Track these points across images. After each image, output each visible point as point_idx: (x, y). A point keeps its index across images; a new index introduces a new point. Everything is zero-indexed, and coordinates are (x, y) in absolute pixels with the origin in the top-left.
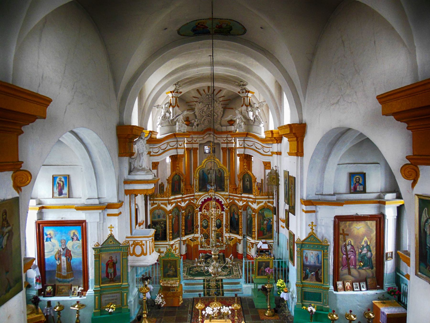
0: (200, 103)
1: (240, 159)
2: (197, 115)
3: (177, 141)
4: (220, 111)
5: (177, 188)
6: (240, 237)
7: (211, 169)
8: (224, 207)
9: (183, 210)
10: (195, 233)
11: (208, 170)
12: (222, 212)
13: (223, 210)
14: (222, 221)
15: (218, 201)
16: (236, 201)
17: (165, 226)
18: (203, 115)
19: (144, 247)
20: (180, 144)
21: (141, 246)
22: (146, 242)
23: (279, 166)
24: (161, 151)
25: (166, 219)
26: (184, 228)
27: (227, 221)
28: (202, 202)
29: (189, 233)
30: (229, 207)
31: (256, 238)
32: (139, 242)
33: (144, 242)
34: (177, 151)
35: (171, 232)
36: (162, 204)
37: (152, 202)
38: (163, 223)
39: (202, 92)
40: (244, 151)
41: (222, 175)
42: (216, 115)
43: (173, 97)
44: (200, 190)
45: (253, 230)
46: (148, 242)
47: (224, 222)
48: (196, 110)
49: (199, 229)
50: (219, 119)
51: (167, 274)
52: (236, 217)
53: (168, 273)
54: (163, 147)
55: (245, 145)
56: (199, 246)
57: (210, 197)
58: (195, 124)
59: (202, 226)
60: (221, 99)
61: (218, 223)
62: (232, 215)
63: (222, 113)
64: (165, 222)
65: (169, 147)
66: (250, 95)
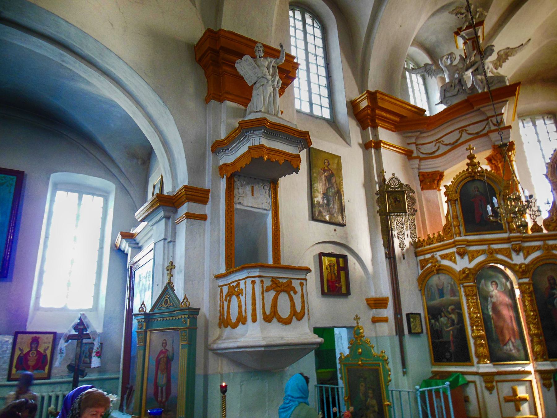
17: (461, 316)
24: (443, 149)
25: (460, 296)
36: (444, 257)
37: (422, 258)
54: (449, 140)
64: (458, 306)
65: (465, 137)
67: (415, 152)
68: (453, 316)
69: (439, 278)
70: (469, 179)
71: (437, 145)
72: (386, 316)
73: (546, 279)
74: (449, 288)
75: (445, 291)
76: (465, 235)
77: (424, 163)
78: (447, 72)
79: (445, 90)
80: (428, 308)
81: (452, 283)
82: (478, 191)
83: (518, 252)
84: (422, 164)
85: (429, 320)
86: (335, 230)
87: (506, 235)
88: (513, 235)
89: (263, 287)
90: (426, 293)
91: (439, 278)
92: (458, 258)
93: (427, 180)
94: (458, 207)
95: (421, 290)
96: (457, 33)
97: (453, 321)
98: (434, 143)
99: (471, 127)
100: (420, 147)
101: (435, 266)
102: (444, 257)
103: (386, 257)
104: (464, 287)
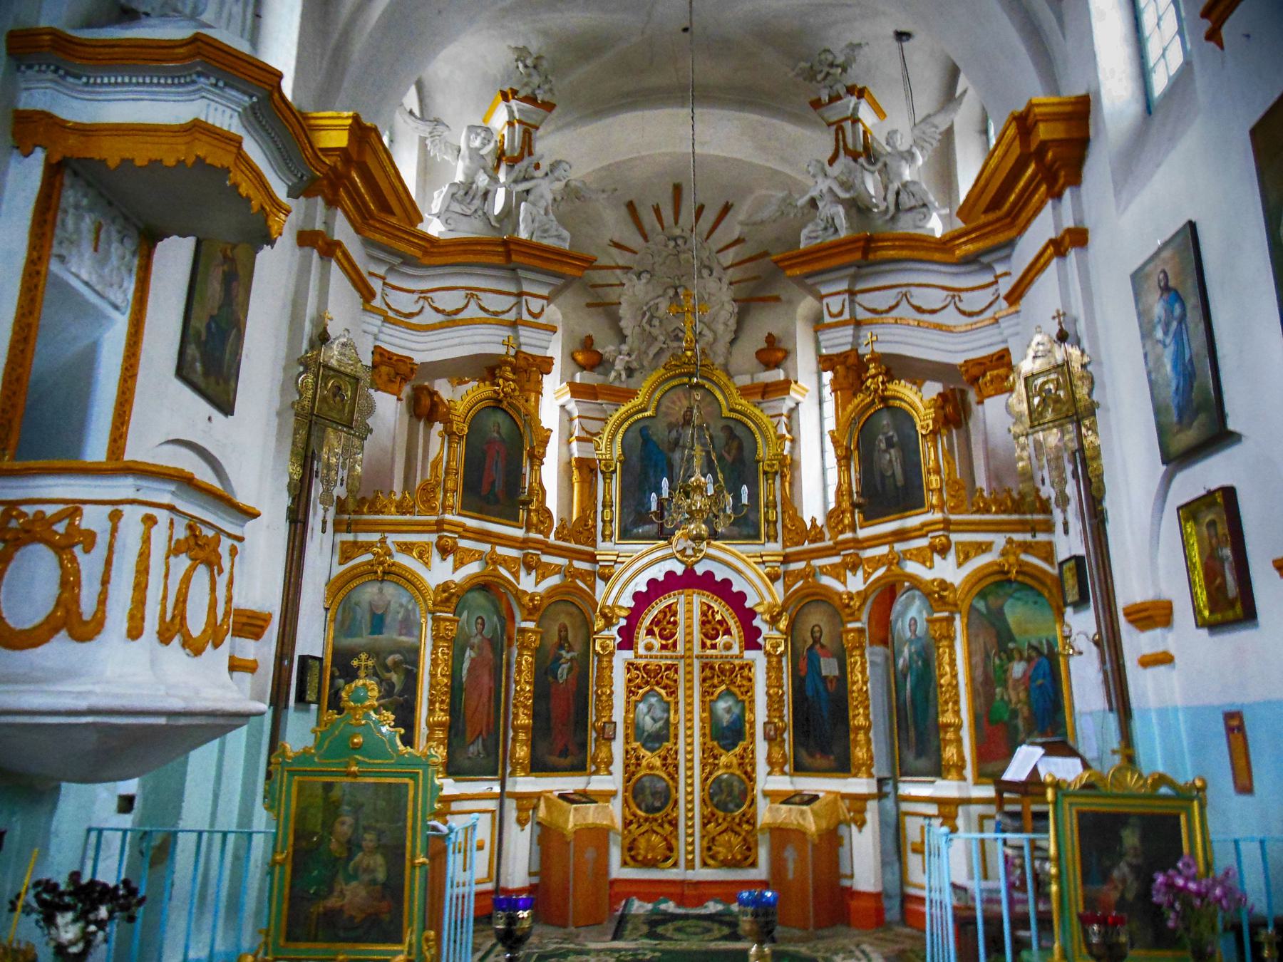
0: (639, 276)
1: (834, 382)
2: (627, 332)
3: (520, 294)
4: (724, 315)
5: (499, 486)
6: (860, 785)
7: (687, 421)
8: (757, 622)
9: (531, 612)
10: (596, 772)
11: (671, 427)
12: (749, 655)
13: (751, 639)
14: (746, 704)
15: (722, 588)
16: (826, 580)
17: (411, 679)
18: (655, 332)
19: (89, 564)
20: (536, 310)
21: (62, 548)
22: (115, 517)
23: (1077, 309)
24: (430, 317)
26: (524, 720)
27: (774, 703)
28: (637, 596)
29: (554, 760)
30: (783, 625)
31: (969, 772)
32: (50, 510)
33: (94, 519)
34: (517, 337)
35: (442, 717)
37: (349, 537)
38: (397, 664)
39: (648, 218)
40: (856, 337)
41: (746, 453)
42: (706, 331)
43: (510, 124)
44: (625, 534)
45: (948, 718)
46: (133, 515)
47: (761, 713)
48: (624, 311)
49: (618, 747)
50: (721, 348)
51: (319, 908)
52: (829, 667)
53: (333, 902)
55: (859, 310)
56: (615, 855)
57: (679, 569)
58: (619, 365)
59: (635, 730)
60: (729, 257)
61: (726, 719)
62: (803, 664)
63: (732, 323)
64: (413, 654)
65: (473, 311)
66: (866, 115)
67: (379, 297)
68: (394, 677)
69: (381, 590)
70: (491, 403)
71: (421, 302)
72: (251, 658)
73: (556, 628)
74: (400, 616)
75: (388, 620)
76: (459, 515)
77: (389, 329)
78: (467, 161)
79: (453, 195)
80: (334, 654)
81: (410, 607)
82: (498, 433)
83: (529, 568)
84: (384, 329)
85: (333, 677)
86: (210, 419)
87: (519, 533)
88: (533, 535)
89: (171, 538)
90: (339, 617)
91: (381, 590)
92: (435, 557)
93: (384, 369)
94: (460, 450)
95: (327, 609)
96: (505, 97)
97: (392, 685)
98: (416, 296)
99: (490, 295)
100: (388, 290)
101: (382, 563)
102: (406, 548)
103: (288, 517)
104: (436, 620)
